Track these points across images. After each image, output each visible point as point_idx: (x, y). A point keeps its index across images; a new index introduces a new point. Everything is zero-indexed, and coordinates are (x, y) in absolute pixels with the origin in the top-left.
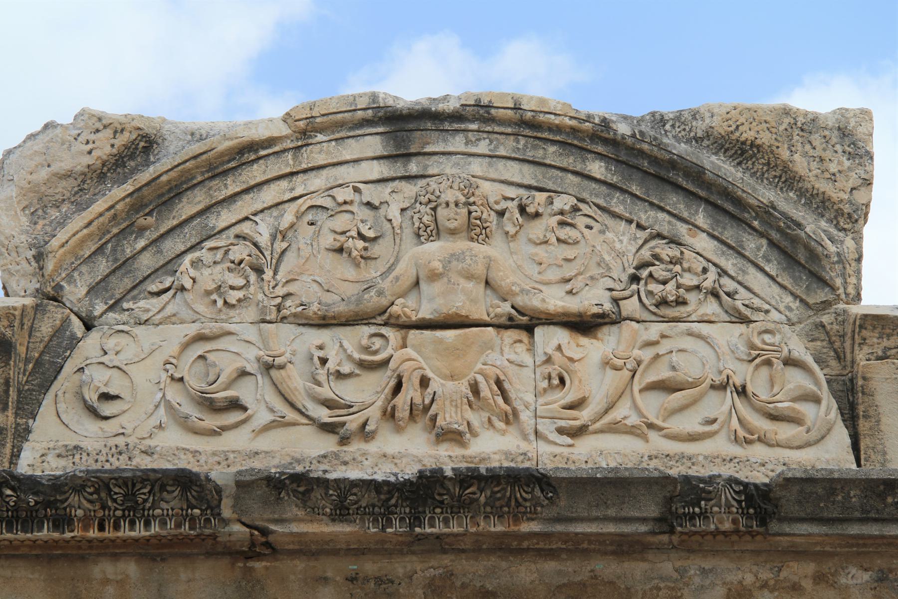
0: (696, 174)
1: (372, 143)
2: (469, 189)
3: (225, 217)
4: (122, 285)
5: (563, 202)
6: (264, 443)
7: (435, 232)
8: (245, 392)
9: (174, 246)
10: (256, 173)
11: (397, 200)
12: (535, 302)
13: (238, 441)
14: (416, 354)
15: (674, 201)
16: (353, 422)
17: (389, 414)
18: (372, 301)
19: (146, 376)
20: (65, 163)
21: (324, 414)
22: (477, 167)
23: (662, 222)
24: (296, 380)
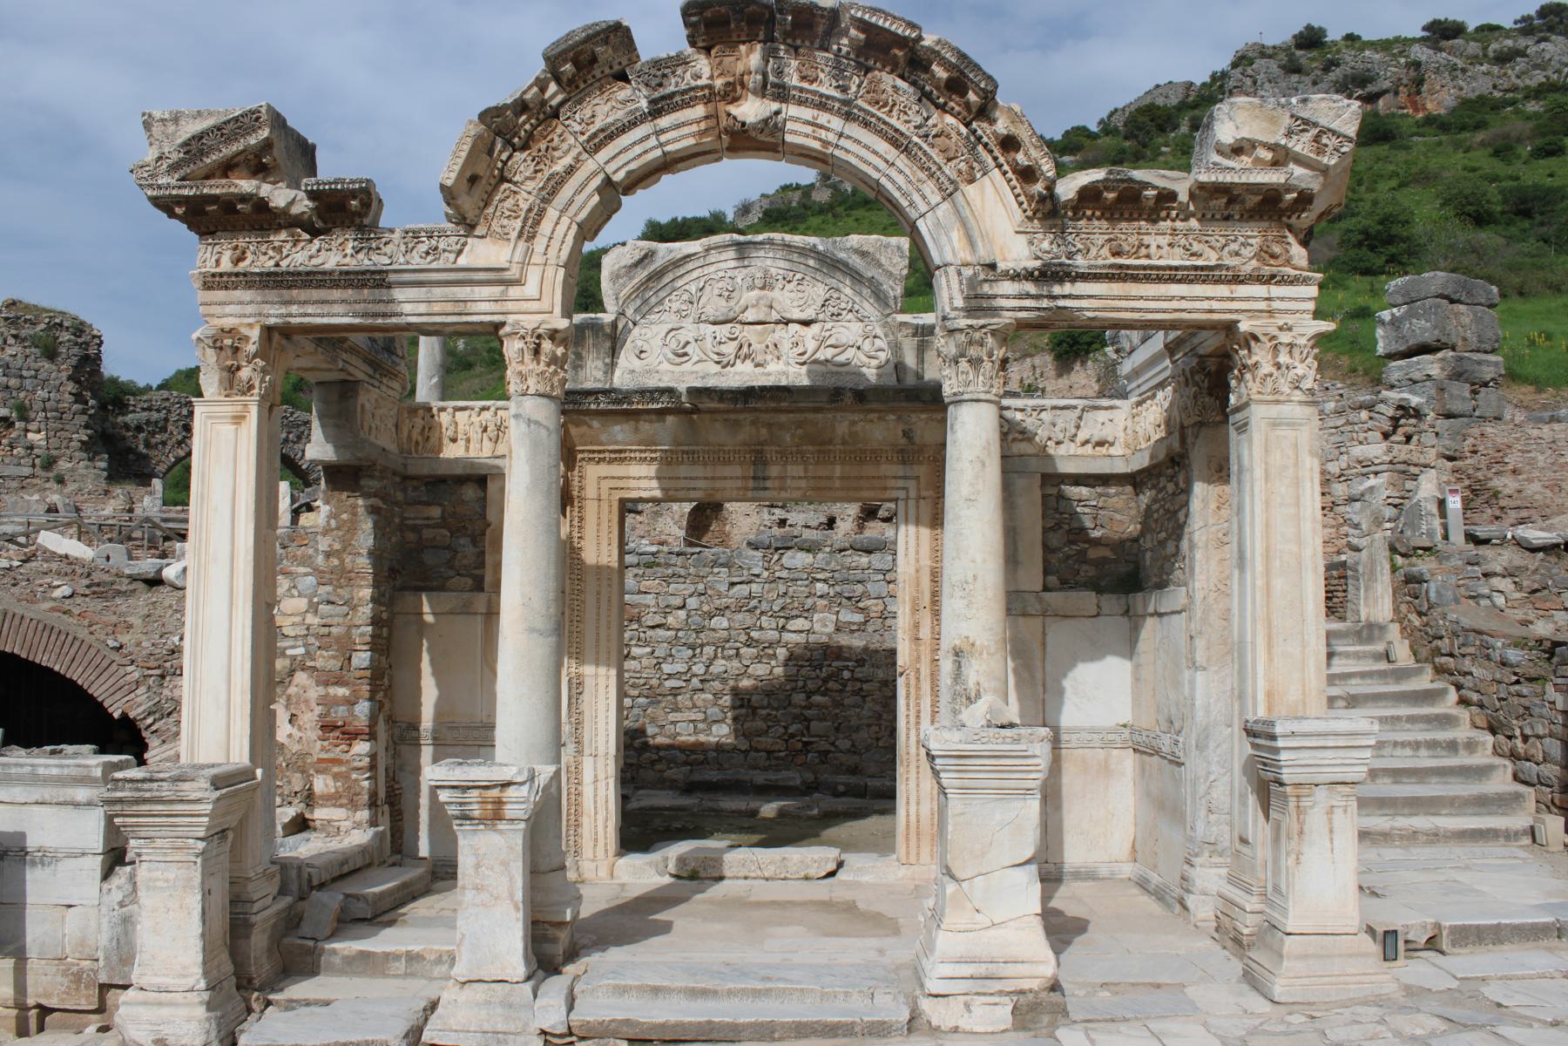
0: (846, 265)
1: (731, 254)
2: (766, 271)
3: (680, 283)
4: (645, 310)
5: (799, 276)
6: (695, 368)
7: (751, 288)
8: (689, 349)
9: (662, 294)
10: (690, 266)
11: (740, 275)
12: (788, 316)
13: (687, 367)
14: (750, 333)
15: (839, 275)
16: (725, 361)
17: (737, 357)
18: (732, 315)
20: (623, 263)
21: (716, 358)
22: (769, 262)
23: (834, 282)
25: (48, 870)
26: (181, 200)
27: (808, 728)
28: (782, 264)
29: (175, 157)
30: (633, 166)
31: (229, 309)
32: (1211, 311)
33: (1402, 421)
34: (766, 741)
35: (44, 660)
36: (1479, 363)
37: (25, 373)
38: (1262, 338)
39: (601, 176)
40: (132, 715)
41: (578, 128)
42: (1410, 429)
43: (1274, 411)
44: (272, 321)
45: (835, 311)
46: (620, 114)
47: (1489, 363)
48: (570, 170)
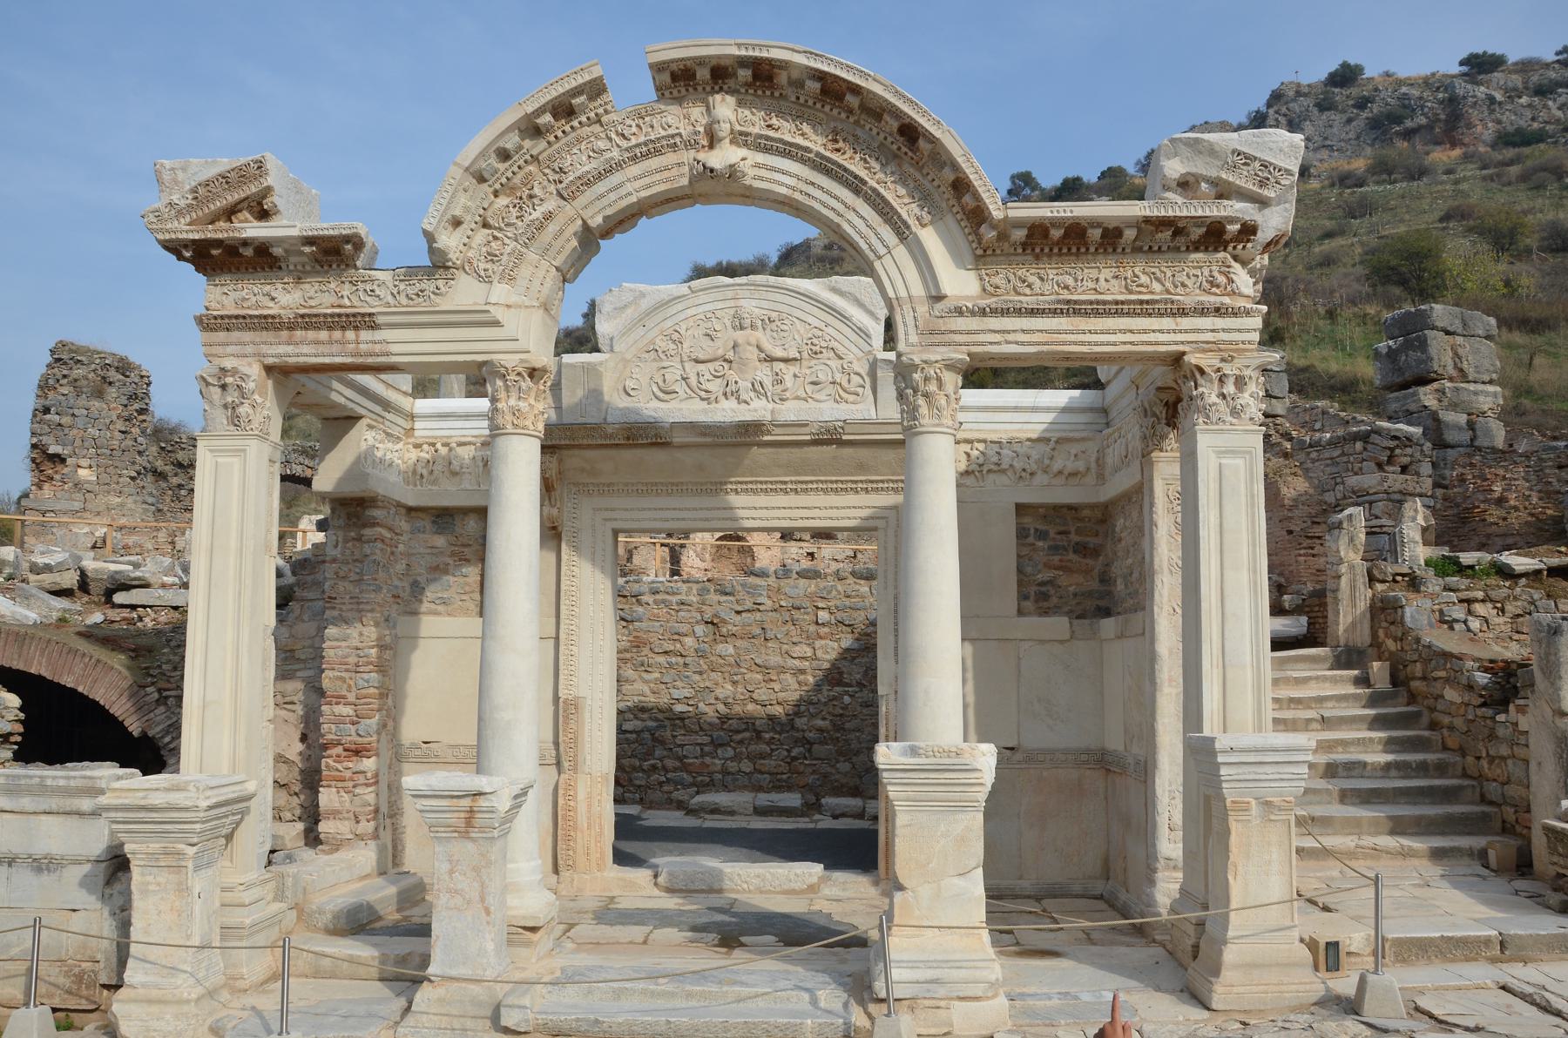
3: (669, 323)
10: (680, 307)
19: (645, 381)
24: (693, 381)
25: (54, 876)
26: (187, 244)
27: (809, 751)
28: (765, 304)
29: (183, 203)
30: (609, 212)
31: (230, 349)
32: (1157, 343)
33: (1398, 451)
34: (769, 764)
35: (68, 681)
36: (1476, 393)
37: (76, 412)
38: (1207, 370)
39: (580, 222)
40: (150, 734)
41: (556, 177)
42: (1406, 460)
43: (1221, 440)
44: (270, 361)
45: (817, 349)
46: (594, 164)
47: (1487, 394)
48: (549, 216)
